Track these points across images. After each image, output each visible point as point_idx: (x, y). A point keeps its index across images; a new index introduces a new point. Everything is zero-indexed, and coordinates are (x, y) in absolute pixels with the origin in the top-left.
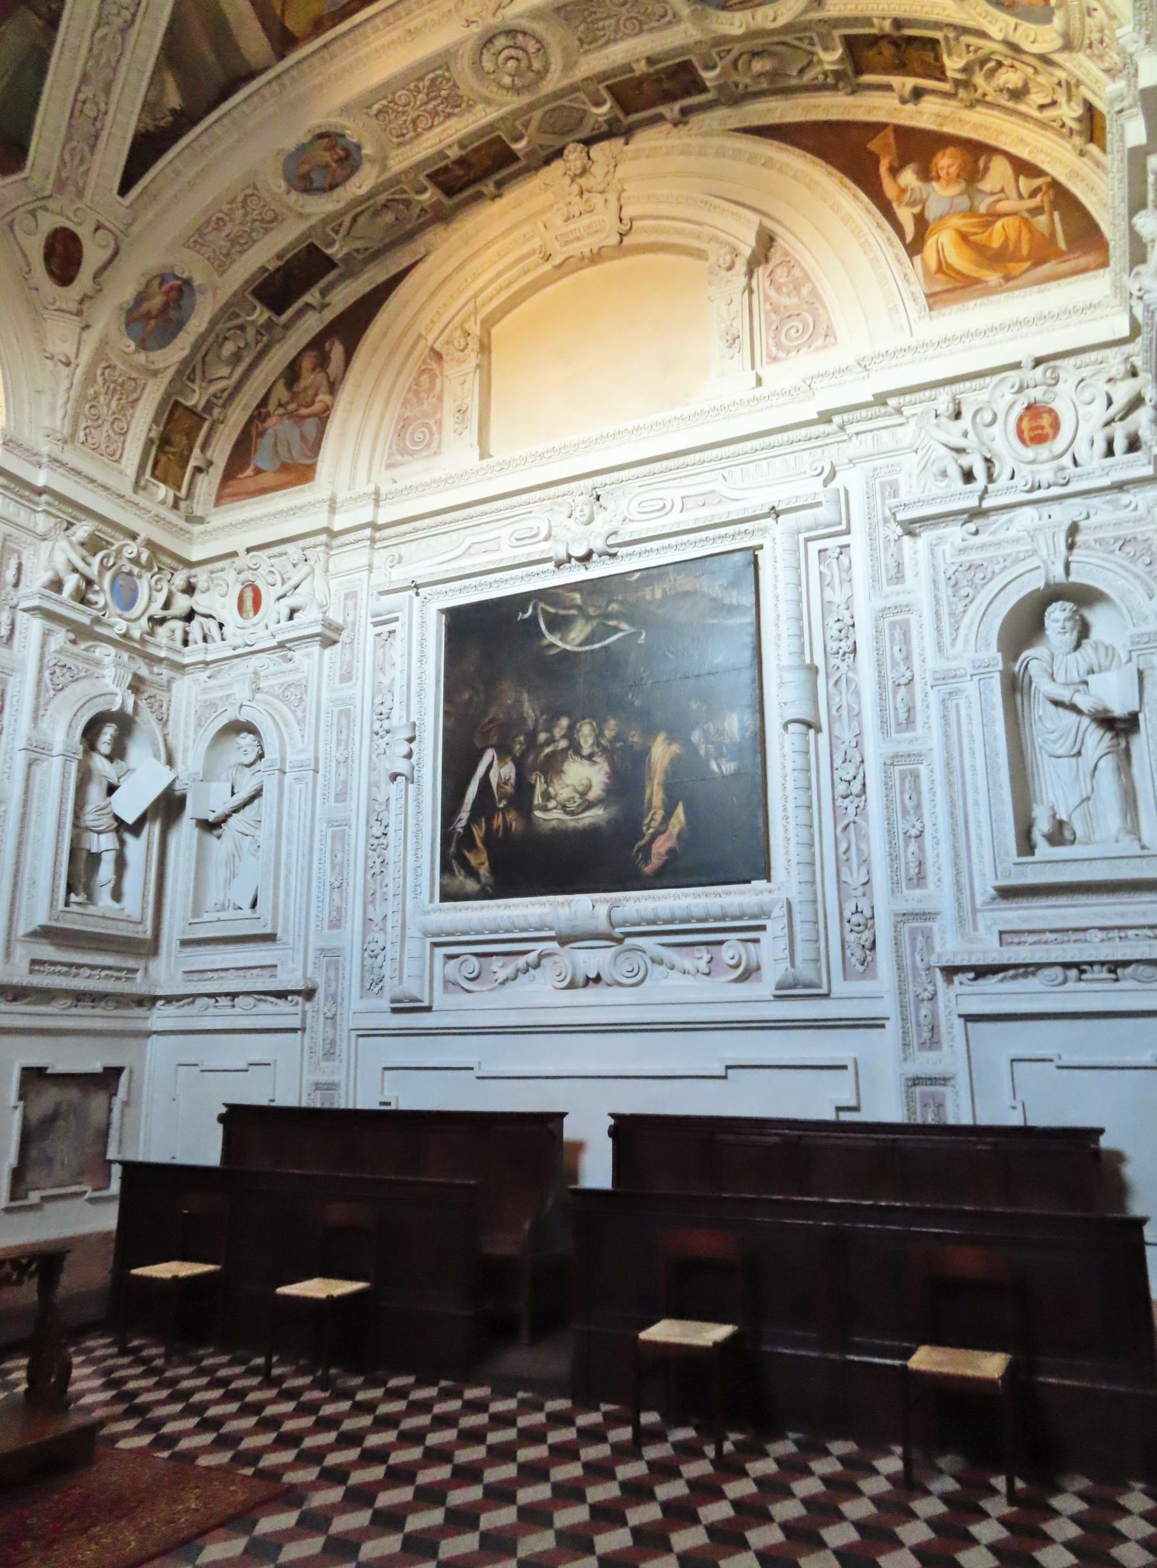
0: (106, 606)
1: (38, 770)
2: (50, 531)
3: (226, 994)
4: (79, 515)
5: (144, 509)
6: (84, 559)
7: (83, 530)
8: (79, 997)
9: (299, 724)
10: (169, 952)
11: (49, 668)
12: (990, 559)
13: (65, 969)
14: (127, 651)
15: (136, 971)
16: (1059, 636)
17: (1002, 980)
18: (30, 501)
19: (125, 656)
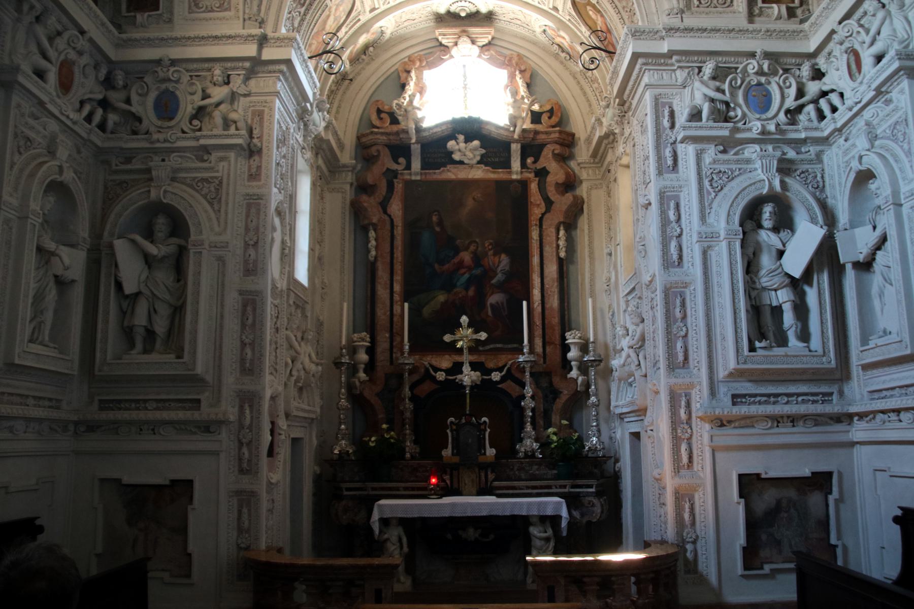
0: (744, 115)
1: (713, 254)
2: (686, 79)
3: (893, 411)
4: (704, 58)
5: (754, 31)
6: (719, 90)
7: (708, 69)
8: (777, 420)
9: (907, 156)
10: (858, 376)
11: (707, 177)
13: (764, 399)
14: (771, 143)
15: (831, 394)
18: (667, 65)
19: (770, 148)
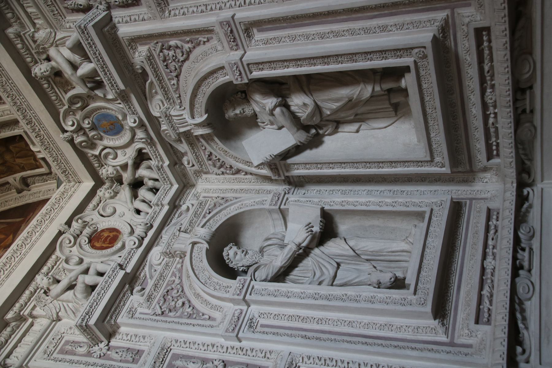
12: (168, 285)
16: (247, 256)
17: (527, 328)
